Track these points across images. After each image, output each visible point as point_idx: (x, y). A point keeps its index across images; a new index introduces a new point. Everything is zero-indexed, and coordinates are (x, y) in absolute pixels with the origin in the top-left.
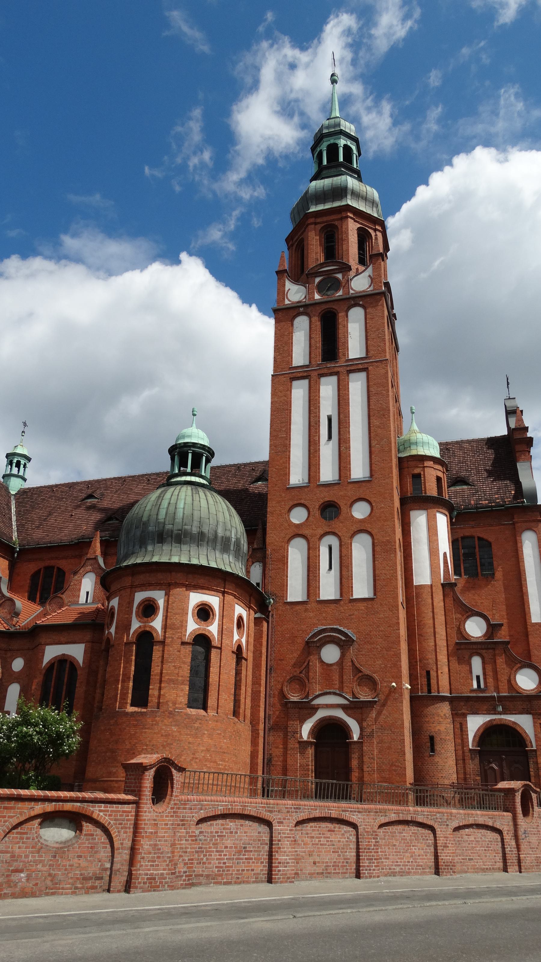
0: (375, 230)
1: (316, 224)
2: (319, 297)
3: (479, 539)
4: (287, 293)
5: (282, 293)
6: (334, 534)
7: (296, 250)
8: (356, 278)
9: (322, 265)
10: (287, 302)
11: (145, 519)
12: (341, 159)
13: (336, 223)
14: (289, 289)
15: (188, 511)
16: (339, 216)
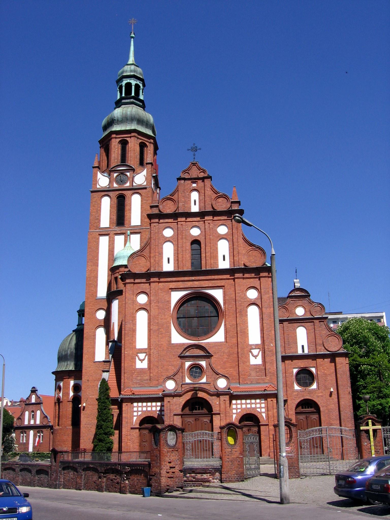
0: (150, 143)
1: (116, 138)
4: (99, 180)
5: (96, 181)
8: (136, 176)
9: (118, 166)
10: (98, 187)
12: (133, 94)
13: (127, 139)
14: (99, 179)
16: (129, 135)
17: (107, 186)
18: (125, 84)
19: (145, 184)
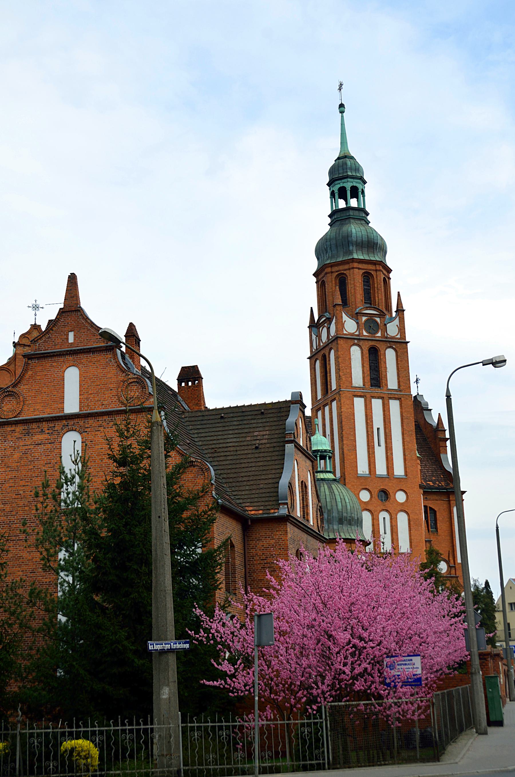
1: (359, 269)
2: (367, 334)
3: (430, 507)
6: (387, 511)
7: (335, 278)
10: (345, 332)
11: (329, 508)
13: (372, 272)
14: (345, 321)
15: (352, 505)
17: (356, 332)
18: (351, 188)
19: (399, 336)
